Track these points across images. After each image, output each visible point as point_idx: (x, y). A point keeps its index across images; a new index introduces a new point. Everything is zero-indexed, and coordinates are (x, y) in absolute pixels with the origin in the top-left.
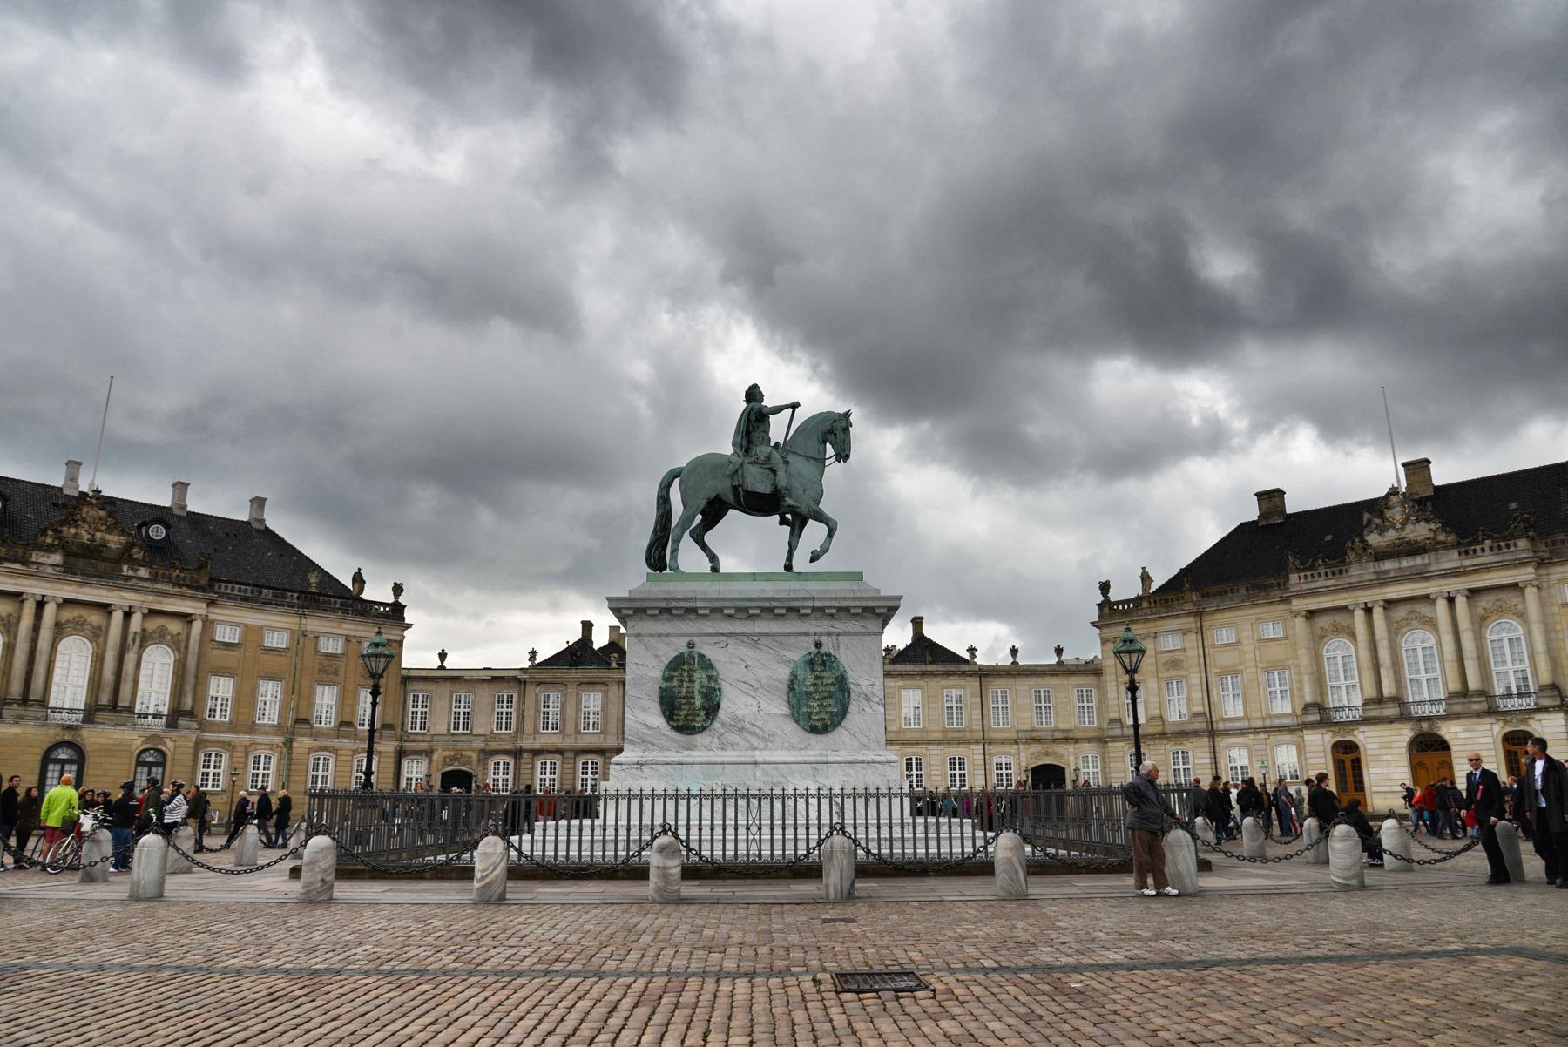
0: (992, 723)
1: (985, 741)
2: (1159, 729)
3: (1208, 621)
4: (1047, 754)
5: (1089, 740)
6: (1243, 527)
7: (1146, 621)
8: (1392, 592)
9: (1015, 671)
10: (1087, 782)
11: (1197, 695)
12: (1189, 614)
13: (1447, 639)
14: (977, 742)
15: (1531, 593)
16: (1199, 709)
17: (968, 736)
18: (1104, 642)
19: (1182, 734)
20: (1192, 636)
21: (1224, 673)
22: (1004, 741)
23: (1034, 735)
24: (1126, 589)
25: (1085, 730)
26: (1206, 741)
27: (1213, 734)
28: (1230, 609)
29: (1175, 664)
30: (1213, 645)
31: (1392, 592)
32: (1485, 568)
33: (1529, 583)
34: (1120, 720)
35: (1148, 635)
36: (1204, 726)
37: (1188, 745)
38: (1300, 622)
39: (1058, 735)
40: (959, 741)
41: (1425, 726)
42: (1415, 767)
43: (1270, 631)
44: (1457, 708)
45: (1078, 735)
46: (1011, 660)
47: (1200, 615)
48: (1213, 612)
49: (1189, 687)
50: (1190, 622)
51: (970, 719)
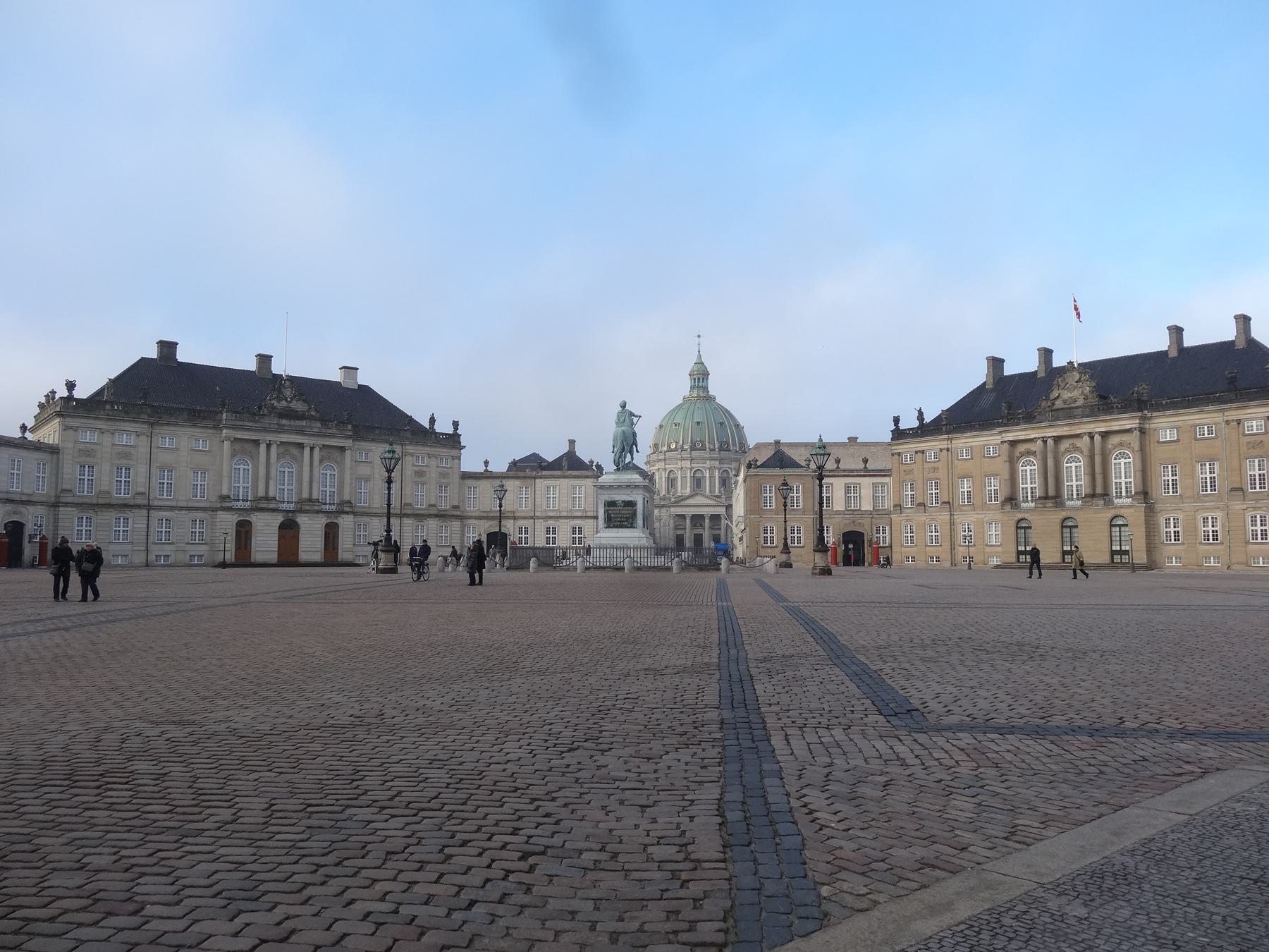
2: (107, 501)
3: (157, 430)
4: (15, 513)
5: (42, 503)
6: (143, 361)
8: (285, 438)
12: (144, 423)
13: (306, 469)
15: (348, 453)
23: (10, 496)
28: (176, 425)
29: (127, 456)
30: (158, 447)
31: (285, 438)
32: (333, 436)
33: (350, 448)
34: (70, 491)
36: (145, 502)
37: (129, 514)
39: (24, 498)
41: (290, 515)
42: (280, 537)
44: (307, 508)
47: (152, 425)
50: (144, 428)
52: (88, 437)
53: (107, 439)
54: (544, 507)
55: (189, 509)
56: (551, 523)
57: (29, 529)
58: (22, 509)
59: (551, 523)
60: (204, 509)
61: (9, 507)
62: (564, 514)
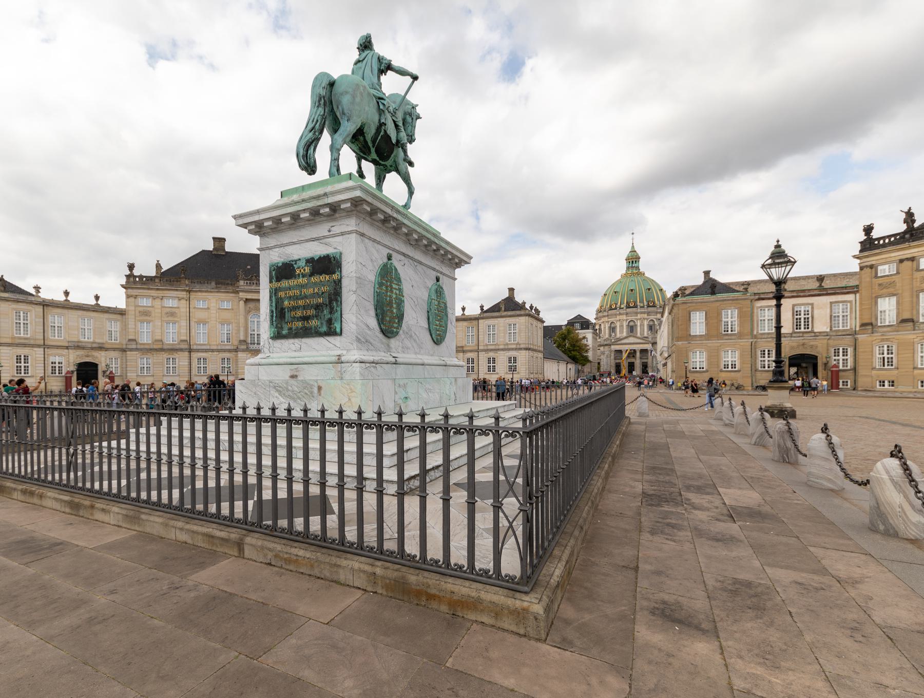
0: (49, 334)
1: (45, 346)
2: (160, 347)
3: (193, 295)
4: (88, 356)
5: (114, 349)
7: (158, 289)
9: (67, 306)
10: (111, 372)
11: (184, 331)
14: (39, 346)
16: (184, 338)
17: (32, 342)
18: (128, 297)
19: (173, 350)
20: (183, 302)
21: (199, 323)
22: (58, 347)
24: (146, 269)
25: (112, 344)
26: (187, 354)
27: (190, 351)
34: (135, 340)
35: (158, 297)
36: (186, 347)
37: (176, 355)
38: (242, 303)
39: (94, 345)
40: (25, 345)
43: (225, 305)
45: (107, 346)
46: (64, 298)
47: (189, 292)
48: (196, 291)
49: (180, 327)
51: (33, 331)
52: (145, 302)
53: (157, 303)
54: (486, 342)
55: (219, 351)
56: (491, 355)
57: (101, 368)
58: (96, 354)
59: (491, 355)
60: (230, 351)
61: (80, 352)
62: (502, 347)
